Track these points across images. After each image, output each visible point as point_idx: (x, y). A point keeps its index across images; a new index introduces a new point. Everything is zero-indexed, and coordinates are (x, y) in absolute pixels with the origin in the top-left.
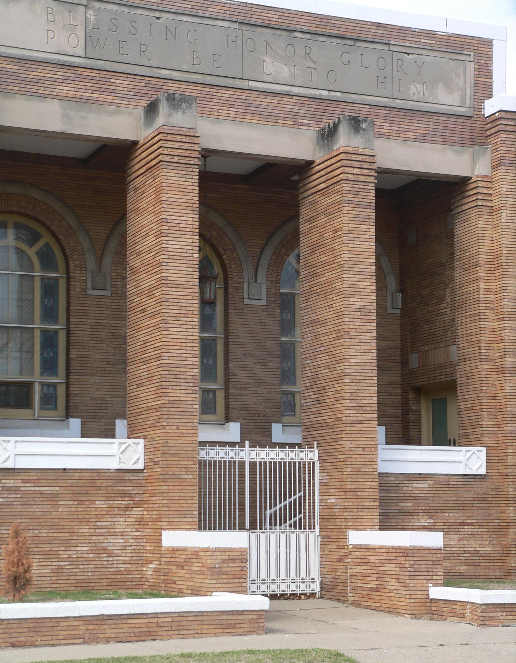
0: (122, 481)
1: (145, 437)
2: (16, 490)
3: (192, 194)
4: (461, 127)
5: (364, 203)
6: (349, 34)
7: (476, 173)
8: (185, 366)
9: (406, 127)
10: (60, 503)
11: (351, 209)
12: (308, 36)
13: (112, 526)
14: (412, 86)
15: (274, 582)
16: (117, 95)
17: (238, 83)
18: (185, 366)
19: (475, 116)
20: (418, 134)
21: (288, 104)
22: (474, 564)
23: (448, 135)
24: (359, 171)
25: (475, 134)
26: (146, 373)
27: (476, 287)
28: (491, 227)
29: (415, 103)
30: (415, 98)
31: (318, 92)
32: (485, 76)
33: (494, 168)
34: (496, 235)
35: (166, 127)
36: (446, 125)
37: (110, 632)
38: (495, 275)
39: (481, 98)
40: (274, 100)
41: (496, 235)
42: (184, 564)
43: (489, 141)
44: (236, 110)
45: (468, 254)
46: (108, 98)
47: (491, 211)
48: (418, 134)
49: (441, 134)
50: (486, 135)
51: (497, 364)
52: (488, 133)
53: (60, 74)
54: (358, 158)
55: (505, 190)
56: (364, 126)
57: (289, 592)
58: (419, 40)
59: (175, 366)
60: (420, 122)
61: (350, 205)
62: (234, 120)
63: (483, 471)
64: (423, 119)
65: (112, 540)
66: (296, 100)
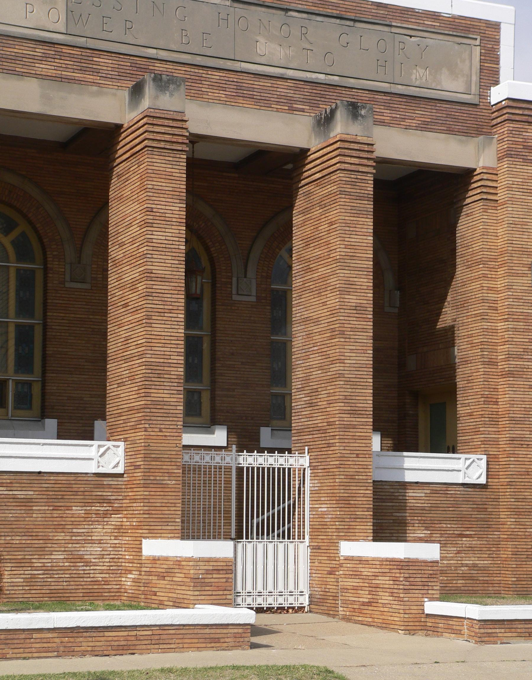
0: (101, 486)
1: (125, 440)
3: (179, 182)
4: (465, 115)
5: (362, 195)
6: (349, 14)
7: (481, 164)
8: (170, 365)
9: (407, 114)
10: (34, 508)
11: (348, 200)
12: (305, 16)
13: (90, 534)
14: (415, 71)
15: (260, 594)
16: (100, 75)
17: (229, 65)
18: (170, 365)
19: (481, 104)
20: (420, 122)
21: (283, 88)
22: (472, 578)
23: (451, 123)
24: (356, 161)
25: (481, 123)
26: (127, 372)
27: (479, 286)
28: (495, 221)
29: (418, 89)
30: (417, 83)
31: (314, 76)
32: (492, 62)
33: (499, 159)
34: (501, 230)
35: (152, 110)
36: (450, 113)
37: (85, 645)
38: (499, 273)
39: (487, 85)
40: (268, 83)
41: (501, 230)
43: (495, 130)
44: (227, 93)
45: (471, 250)
46: (90, 78)
47: (496, 205)
48: (420, 122)
49: (444, 122)
50: (491, 124)
51: (500, 367)
52: (494, 122)
53: (40, 50)
54: (356, 146)
55: (511, 182)
56: (363, 112)
57: (276, 606)
58: (422, 22)
59: (158, 364)
60: (423, 109)
61: (347, 197)
62: (225, 103)
63: (483, 480)
64: (426, 107)
65: (89, 548)
66: (290, 83)
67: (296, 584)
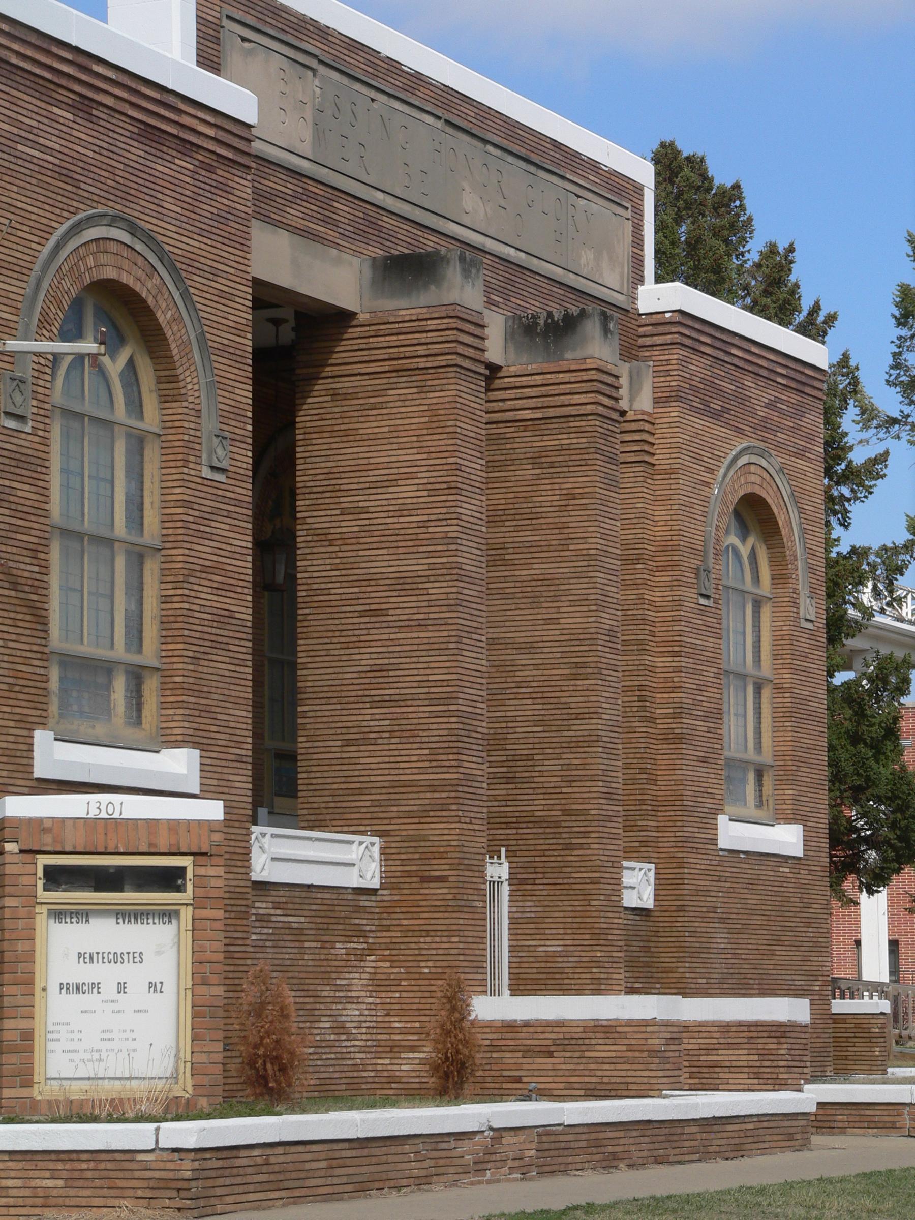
1: (380, 834)
10: (307, 944)
26: (387, 722)
42: (552, 1048)
51: (660, 726)
52: (641, 341)
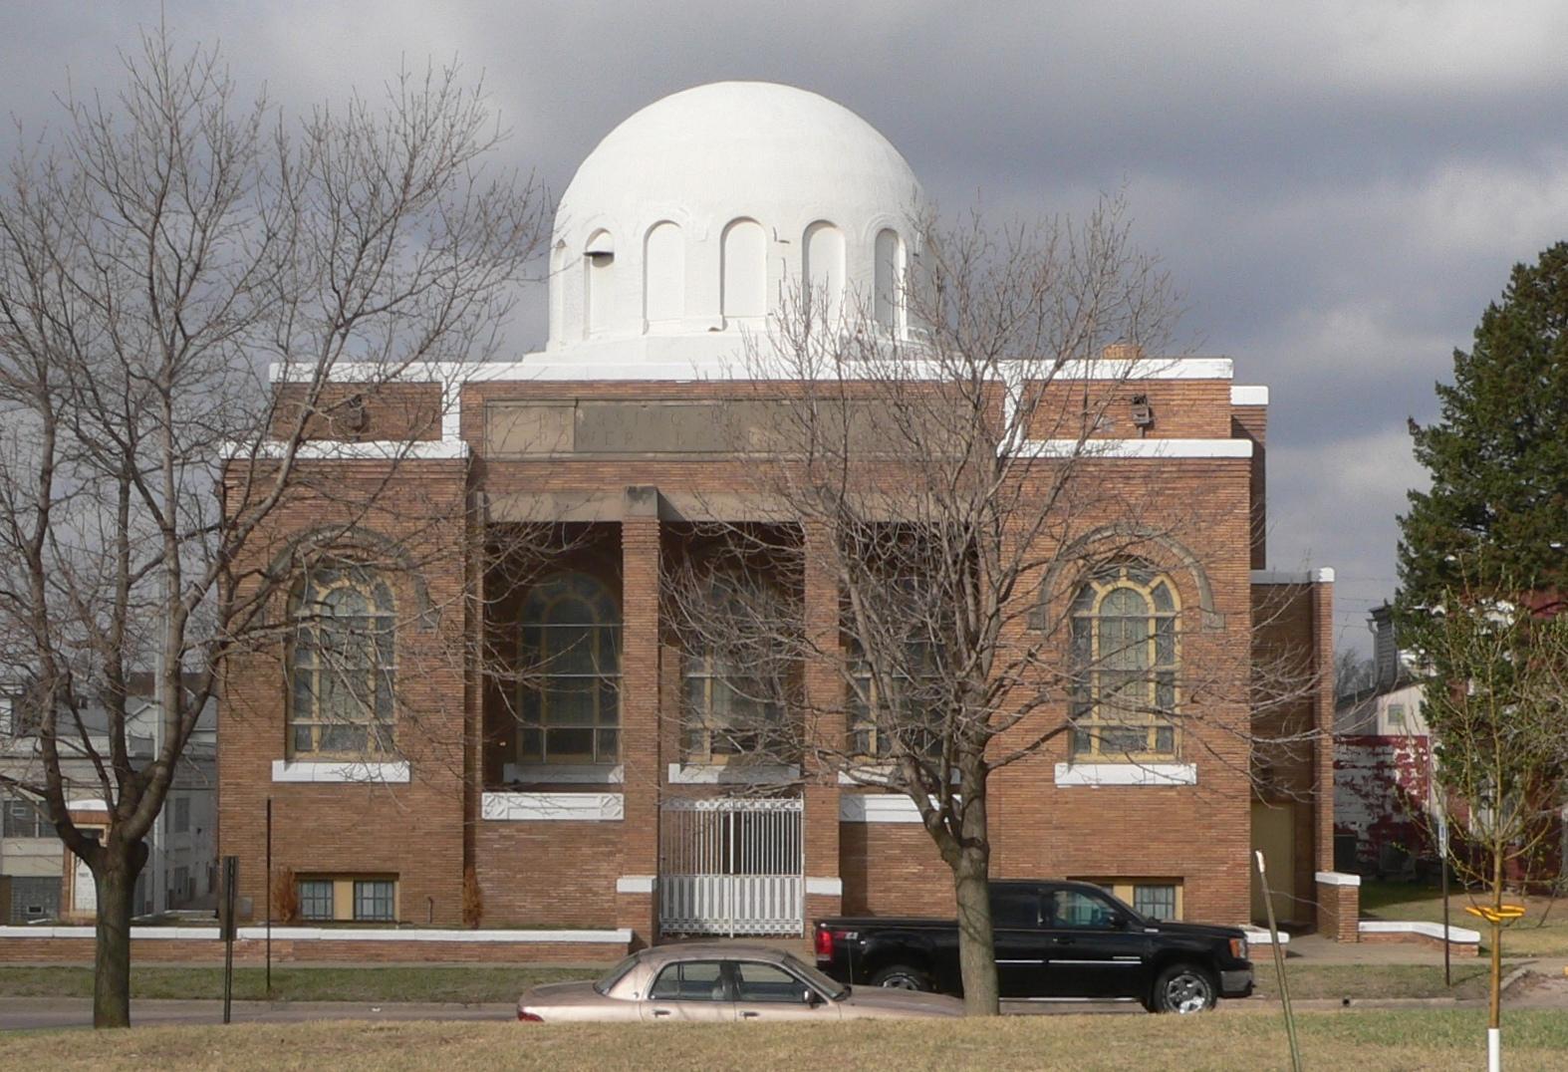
2: (511, 838)
65: (597, 881)
67: (793, 915)
